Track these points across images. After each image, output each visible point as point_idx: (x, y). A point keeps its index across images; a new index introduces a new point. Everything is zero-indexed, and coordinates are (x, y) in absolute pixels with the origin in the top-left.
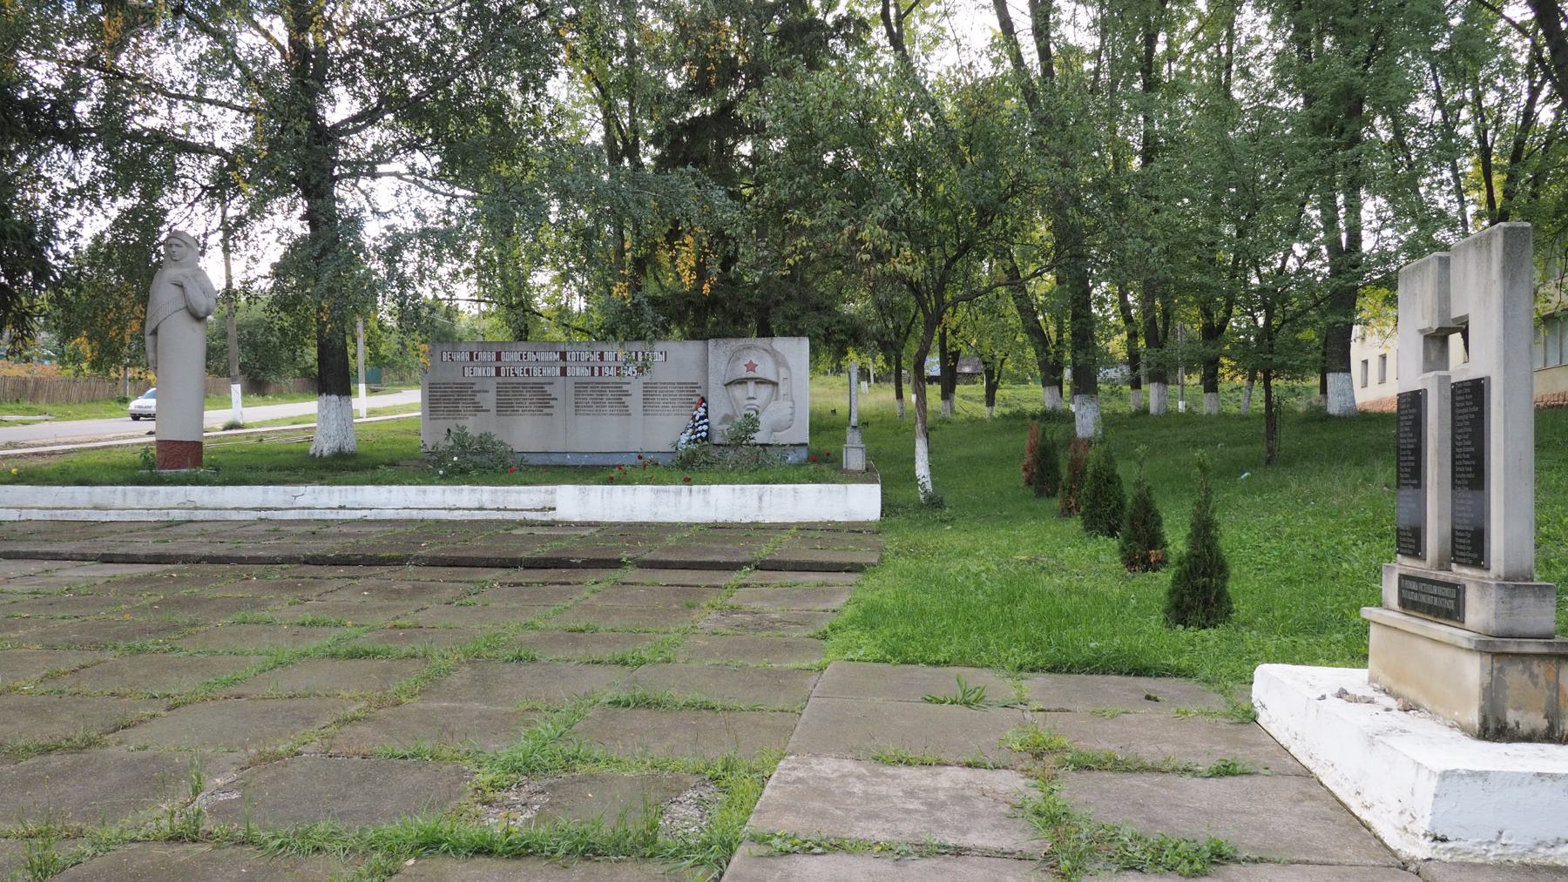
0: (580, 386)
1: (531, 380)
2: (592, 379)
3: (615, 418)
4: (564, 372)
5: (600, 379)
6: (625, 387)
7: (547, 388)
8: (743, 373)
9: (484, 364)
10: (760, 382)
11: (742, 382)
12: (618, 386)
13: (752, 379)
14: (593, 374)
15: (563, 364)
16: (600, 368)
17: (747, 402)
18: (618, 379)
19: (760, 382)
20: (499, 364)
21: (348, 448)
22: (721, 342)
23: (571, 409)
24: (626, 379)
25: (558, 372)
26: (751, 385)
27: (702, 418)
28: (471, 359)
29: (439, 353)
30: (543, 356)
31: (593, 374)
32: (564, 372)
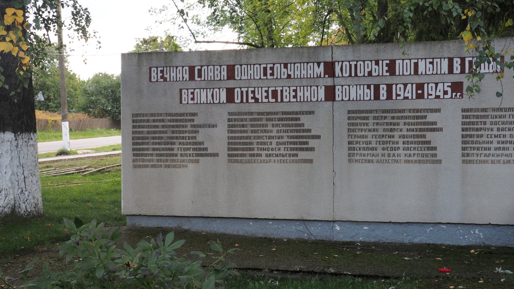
1: (280, 108)
2: (375, 105)
5: (389, 105)
6: (431, 117)
7: (304, 119)
14: (377, 97)
15: (329, 82)
16: (389, 87)
18: (421, 104)
20: (231, 84)
21: (23, 208)
23: (343, 152)
28: (192, 77)
29: (145, 69)
31: (377, 97)
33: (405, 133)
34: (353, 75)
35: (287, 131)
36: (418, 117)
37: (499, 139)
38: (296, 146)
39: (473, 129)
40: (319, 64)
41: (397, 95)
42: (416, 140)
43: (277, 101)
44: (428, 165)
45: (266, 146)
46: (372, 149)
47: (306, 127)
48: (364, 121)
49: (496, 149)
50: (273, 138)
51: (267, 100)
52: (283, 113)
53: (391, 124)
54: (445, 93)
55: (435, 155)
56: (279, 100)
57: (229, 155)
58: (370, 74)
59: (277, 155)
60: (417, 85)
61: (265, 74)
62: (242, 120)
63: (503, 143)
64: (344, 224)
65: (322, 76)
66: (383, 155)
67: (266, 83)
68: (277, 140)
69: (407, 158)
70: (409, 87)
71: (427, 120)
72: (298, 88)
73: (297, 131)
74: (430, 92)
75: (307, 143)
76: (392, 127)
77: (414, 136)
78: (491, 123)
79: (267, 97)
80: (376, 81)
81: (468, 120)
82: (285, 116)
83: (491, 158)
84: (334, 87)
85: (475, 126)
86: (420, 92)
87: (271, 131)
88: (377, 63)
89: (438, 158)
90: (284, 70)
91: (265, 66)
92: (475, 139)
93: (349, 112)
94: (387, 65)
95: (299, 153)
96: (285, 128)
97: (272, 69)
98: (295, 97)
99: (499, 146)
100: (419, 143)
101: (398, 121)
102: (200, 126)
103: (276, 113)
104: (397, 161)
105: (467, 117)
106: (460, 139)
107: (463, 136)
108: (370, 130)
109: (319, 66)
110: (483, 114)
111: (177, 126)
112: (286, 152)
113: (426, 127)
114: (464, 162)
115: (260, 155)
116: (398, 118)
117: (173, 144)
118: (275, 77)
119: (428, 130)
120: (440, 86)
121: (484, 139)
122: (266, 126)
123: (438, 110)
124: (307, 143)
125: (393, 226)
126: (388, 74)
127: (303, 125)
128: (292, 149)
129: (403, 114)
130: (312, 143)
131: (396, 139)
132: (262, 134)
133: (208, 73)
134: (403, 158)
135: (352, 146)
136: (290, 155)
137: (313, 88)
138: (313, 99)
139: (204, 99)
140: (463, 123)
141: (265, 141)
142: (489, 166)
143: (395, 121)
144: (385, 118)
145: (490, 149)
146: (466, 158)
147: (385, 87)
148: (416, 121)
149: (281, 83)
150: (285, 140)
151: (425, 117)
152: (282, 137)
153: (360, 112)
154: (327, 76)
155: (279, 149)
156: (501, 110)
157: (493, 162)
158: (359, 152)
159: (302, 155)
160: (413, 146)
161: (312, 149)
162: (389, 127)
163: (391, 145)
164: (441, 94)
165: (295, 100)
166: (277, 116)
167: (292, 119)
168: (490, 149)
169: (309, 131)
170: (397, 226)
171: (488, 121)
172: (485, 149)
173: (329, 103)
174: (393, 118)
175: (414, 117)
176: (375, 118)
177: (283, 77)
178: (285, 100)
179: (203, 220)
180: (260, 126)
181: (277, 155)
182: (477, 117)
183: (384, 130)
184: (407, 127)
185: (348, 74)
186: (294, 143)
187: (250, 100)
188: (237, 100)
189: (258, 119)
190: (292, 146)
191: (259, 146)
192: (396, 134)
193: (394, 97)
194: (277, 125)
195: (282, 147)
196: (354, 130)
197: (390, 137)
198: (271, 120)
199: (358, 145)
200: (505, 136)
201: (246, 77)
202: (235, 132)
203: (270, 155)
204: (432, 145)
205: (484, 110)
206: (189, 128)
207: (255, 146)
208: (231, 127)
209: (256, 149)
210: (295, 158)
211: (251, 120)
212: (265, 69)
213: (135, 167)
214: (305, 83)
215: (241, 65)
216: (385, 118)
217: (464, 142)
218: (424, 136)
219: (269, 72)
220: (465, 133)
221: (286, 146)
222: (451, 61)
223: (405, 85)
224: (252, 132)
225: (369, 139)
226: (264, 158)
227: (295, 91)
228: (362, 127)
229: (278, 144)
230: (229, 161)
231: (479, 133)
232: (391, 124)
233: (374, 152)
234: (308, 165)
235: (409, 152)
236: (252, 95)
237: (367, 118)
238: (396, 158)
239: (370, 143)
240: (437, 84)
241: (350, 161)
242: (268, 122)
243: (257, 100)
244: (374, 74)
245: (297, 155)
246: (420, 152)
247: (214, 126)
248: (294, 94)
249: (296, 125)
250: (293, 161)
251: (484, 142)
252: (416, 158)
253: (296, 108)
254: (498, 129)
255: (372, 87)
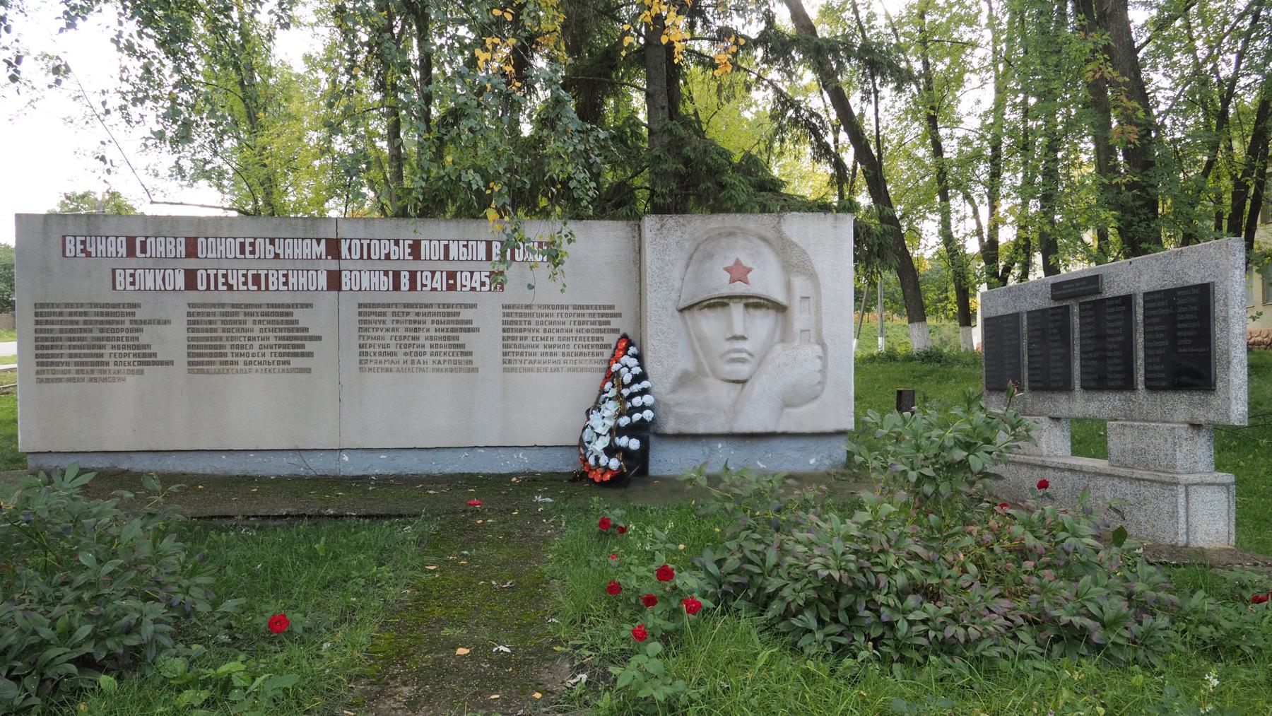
0: (369, 311)
1: (264, 298)
2: (395, 297)
3: (446, 378)
4: (335, 281)
5: (412, 298)
6: (465, 314)
7: (298, 314)
8: (722, 284)
9: (159, 264)
10: (756, 303)
11: (720, 303)
12: (450, 311)
13: (741, 297)
14: (397, 287)
15: (333, 265)
16: (413, 275)
17: (728, 346)
18: (452, 297)
19: (756, 303)
20: (192, 264)
22: (671, 220)
24: (470, 298)
25: (323, 281)
26: (737, 310)
27: (637, 379)
28: (131, 252)
30: (289, 249)
31: (397, 287)
32: (335, 281)
33: (433, 334)
34: (365, 256)
35: (274, 330)
36: (449, 314)
37: (546, 343)
38: (287, 351)
39: (516, 330)
40: (319, 241)
41: (423, 285)
42: (447, 342)
43: (259, 289)
44: (463, 375)
45: (245, 351)
46: (391, 354)
47: (301, 325)
48: (380, 318)
49: (542, 354)
50: (254, 339)
51: (245, 288)
52: (269, 305)
53: (415, 322)
54: (483, 284)
55: (471, 362)
56: (263, 288)
57: (190, 363)
58: (388, 256)
59: (260, 363)
60: (448, 273)
61: (243, 252)
62: (208, 314)
63: (550, 347)
64: (354, 453)
65: (324, 257)
66: (405, 362)
67: (244, 264)
68: (260, 342)
69: (436, 366)
70: (438, 275)
71: (460, 318)
72: (290, 272)
73: (289, 330)
74: (464, 283)
75: (303, 346)
76: (417, 326)
77: (444, 338)
78: (537, 323)
79: (245, 283)
80: (396, 266)
81: (510, 319)
82: (271, 310)
83: (537, 365)
84: (340, 272)
85: (519, 327)
86: (451, 282)
87: (252, 330)
88: (397, 243)
89: (474, 365)
90: (269, 247)
91: (242, 240)
92: (518, 342)
93: (360, 306)
94: (410, 246)
95: (292, 360)
96: (271, 326)
97: (252, 244)
98: (286, 284)
99: (546, 350)
100: (450, 346)
101: (424, 318)
102: (145, 322)
103: (260, 306)
104: (422, 370)
105: (508, 315)
106: (500, 343)
107: (504, 339)
108: (388, 330)
109: (319, 244)
110: (527, 311)
111: (109, 322)
112: (274, 358)
113: (459, 326)
114: (504, 369)
115: (237, 363)
116: (424, 314)
117: (103, 347)
118: (257, 256)
119: (461, 330)
120: (476, 275)
121: (529, 342)
122: (245, 322)
123: (474, 306)
124: (303, 346)
125: (418, 452)
126: (411, 258)
127: (297, 322)
128: (282, 355)
129: (431, 310)
130: (310, 346)
131: (421, 342)
132: (239, 334)
133: (157, 247)
134: (430, 365)
135: (364, 350)
136: (278, 363)
137: (310, 273)
138: (310, 288)
139: (150, 284)
140: (504, 323)
141: (243, 343)
142: (534, 374)
143: (421, 318)
144: (408, 314)
145: (535, 354)
146: (507, 366)
147: (407, 274)
148: (446, 318)
149: (265, 264)
150: (272, 342)
151: (458, 314)
152: (268, 338)
153: (374, 305)
154: (329, 257)
155: (264, 355)
156: (548, 307)
157: (539, 370)
158: (373, 358)
159: (296, 362)
160: (443, 350)
161: (310, 354)
162: (413, 326)
163: (415, 350)
164: (477, 285)
165: (286, 288)
166: (259, 310)
167: (282, 314)
168: (535, 354)
169: (306, 330)
170: (424, 453)
171: (533, 320)
172: (530, 354)
173: (334, 294)
174: (418, 314)
175: (444, 314)
176: (394, 314)
177: (268, 256)
178: (271, 288)
179: (147, 454)
180: (235, 322)
181: (260, 363)
182: (521, 315)
183: (406, 330)
184: (435, 325)
185: (358, 256)
186: (284, 347)
187: (221, 287)
188: (202, 286)
189: (233, 314)
190: (282, 350)
191: (236, 351)
192: (422, 335)
193: (419, 288)
194: (260, 322)
195: (268, 351)
196: (366, 330)
197: (414, 338)
198: (252, 314)
199: (372, 349)
200: (552, 339)
201: (214, 255)
202: (198, 331)
203: (250, 363)
204: (466, 349)
205: (528, 307)
206: (127, 325)
207: (228, 350)
208: (192, 325)
209: (230, 355)
210: (286, 366)
211: (223, 314)
212: (242, 245)
213: (40, 381)
214: (299, 265)
215: (207, 238)
216: (408, 314)
217: (505, 346)
218: (457, 338)
219: (248, 249)
220: (506, 334)
221: (274, 350)
222: (489, 244)
223: (433, 273)
224: (224, 330)
225: (387, 341)
226: (241, 366)
227: (286, 276)
228: (378, 326)
229: (261, 347)
230: (190, 371)
231: (523, 334)
232: (415, 322)
233: (394, 358)
234: (305, 376)
235: (438, 358)
236: (224, 280)
237: (384, 314)
238: (422, 366)
239: (388, 346)
240: (472, 273)
241: (361, 369)
242: (247, 318)
243: (230, 287)
244: (392, 257)
245: (289, 363)
246: (452, 358)
247: (166, 322)
248: (284, 280)
249: (287, 322)
250: (283, 370)
251: (528, 346)
252: (446, 365)
253: (287, 299)
254: (545, 331)
255: (391, 273)
